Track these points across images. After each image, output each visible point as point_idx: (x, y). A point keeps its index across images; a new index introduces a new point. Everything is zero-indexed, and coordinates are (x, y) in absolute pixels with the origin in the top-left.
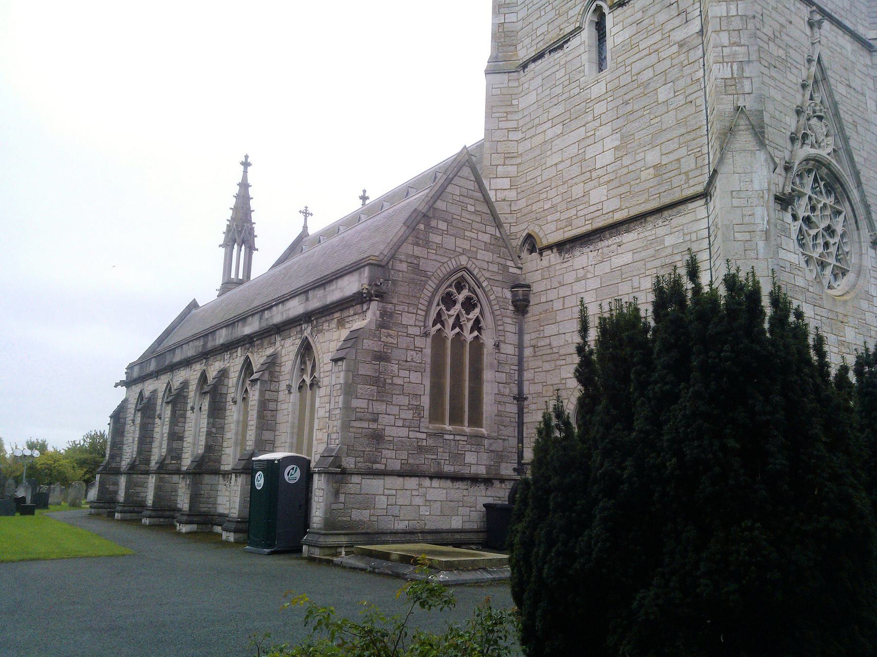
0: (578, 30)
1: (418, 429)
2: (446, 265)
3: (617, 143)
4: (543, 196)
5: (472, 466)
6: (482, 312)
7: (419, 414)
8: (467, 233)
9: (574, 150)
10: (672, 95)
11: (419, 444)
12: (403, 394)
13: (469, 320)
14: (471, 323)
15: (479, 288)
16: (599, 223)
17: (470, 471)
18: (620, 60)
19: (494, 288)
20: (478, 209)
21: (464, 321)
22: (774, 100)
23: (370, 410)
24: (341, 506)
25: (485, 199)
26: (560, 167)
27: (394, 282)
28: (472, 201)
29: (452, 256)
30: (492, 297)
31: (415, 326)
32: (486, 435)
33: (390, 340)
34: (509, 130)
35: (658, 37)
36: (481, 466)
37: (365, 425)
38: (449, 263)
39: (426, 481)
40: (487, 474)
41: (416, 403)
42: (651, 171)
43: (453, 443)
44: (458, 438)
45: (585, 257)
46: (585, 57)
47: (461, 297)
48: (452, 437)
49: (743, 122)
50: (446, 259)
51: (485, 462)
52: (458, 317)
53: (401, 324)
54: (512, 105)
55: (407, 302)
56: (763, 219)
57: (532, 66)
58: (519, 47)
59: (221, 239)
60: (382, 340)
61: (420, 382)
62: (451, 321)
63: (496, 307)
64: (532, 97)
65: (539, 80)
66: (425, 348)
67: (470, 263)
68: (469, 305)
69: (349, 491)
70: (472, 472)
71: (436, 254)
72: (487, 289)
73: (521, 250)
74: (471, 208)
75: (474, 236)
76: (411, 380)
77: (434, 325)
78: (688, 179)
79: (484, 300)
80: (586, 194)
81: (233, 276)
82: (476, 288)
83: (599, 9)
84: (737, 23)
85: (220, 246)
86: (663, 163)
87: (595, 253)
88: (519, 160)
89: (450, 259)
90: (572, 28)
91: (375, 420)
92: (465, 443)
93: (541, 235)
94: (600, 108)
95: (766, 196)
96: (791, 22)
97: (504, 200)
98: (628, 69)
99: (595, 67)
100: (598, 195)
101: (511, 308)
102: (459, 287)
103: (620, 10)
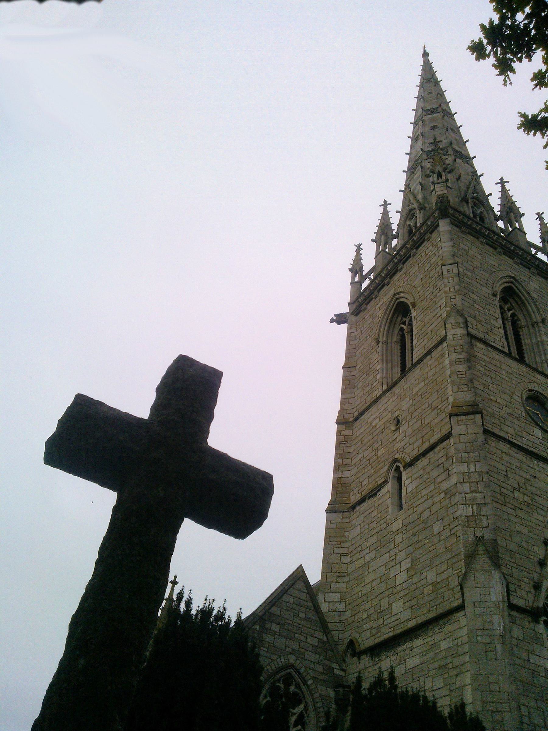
0: (386, 482)
2: (275, 662)
3: (410, 565)
4: (362, 608)
8: (297, 636)
9: (382, 570)
10: (442, 529)
15: (304, 685)
16: (399, 630)
18: (410, 503)
19: (318, 686)
20: (309, 616)
22: (521, 533)
25: (315, 608)
26: (374, 584)
28: (303, 609)
29: (281, 655)
30: (316, 695)
34: (341, 555)
35: (432, 487)
38: (279, 660)
42: (431, 587)
45: (388, 660)
46: (389, 502)
49: (481, 548)
54: (344, 536)
56: (500, 626)
57: (358, 507)
58: (351, 494)
63: (319, 704)
64: (358, 531)
65: (362, 517)
67: (298, 662)
71: (268, 652)
72: (311, 687)
74: (302, 615)
75: (303, 638)
78: (454, 593)
80: (390, 606)
83: (398, 468)
84: (475, 477)
86: (438, 581)
87: (395, 657)
88: (347, 579)
89: (280, 657)
90: (382, 480)
93: (360, 641)
94: (398, 538)
95: (501, 607)
96: (535, 477)
97: (335, 611)
98: (415, 510)
99: (396, 508)
100: (397, 607)
103: (410, 469)
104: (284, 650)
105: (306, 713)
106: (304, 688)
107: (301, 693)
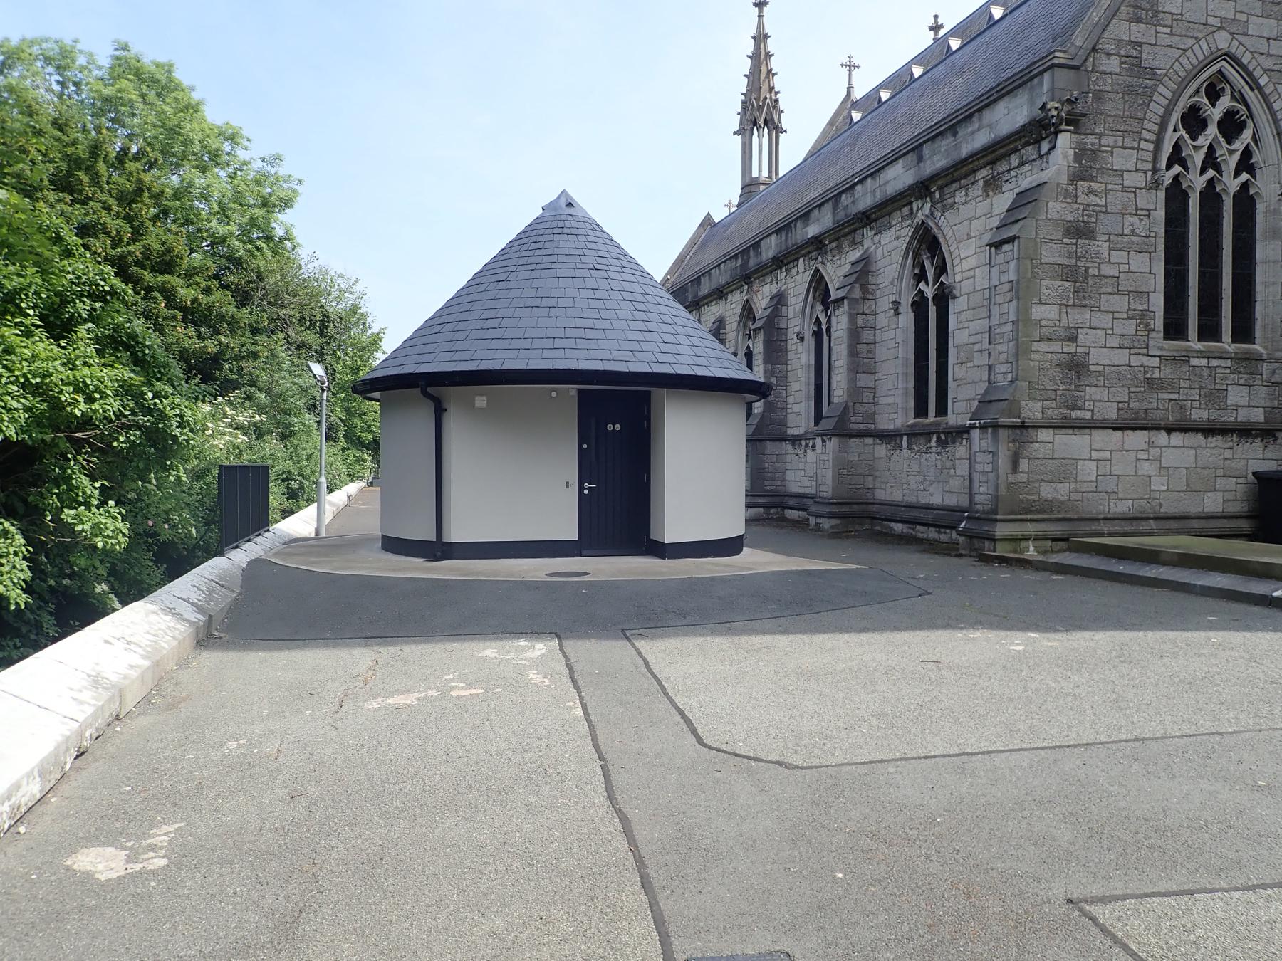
1: (1145, 351)
2: (1189, 53)
5: (1240, 409)
6: (1255, 138)
7: (1147, 325)
11: (1148, 376)
12: (1118, 292)
13: (1231, 152)
14: (1237, 156)
15: (1252, 90)
17: (1236, 418)
21: (1222, 155)
23: (1064, 323)
24: (1024, 477)
27: (1098, 96)
29: (1200, 35)
31: (1137, 171)
32: (1265, 357)
33: (1093, 199)
36: (1256, 409)
37: (1056, 347)
38: (1196, 47)
39: (1160, 436)
40: (1266, 422)
41: (1140, 307)
43: (1206, 372)
44: (1214, 363)
47: (1216, 113)
48: (1204, 362)
51: (1263, 403)
52: (1211, 149)
53: (1112, 170)
55: (1122, 128)
59: (735, 123)
60: (1079, 201)
61: (1148, 271)
62: (1199, 157)
66: (1155, 209)
67: (1235, 43)
68: (1231, 126)
69: (1034, 454)
70: (1239, 420)
71: (1171, 34)
72: (1267, 91)
77: (1169, 167)
81: (755, 174)
85: (735, 133)
89: (1198, 40)
91: (1073, 339)
92: (1228, 371)
102: (1213, 94)
104: (1204, 25)
105: (1257, 145)
106: (1251, 96)
107: (1244, 108)
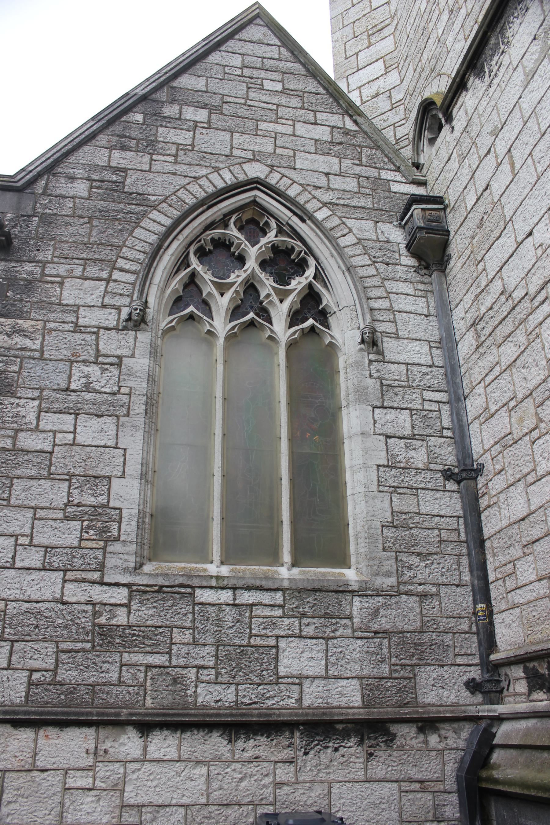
1: (96, 576)
2: (202, 182)
5: (306, 683)
7: (105, 530)
11: (102, 620)
12: (50, 476)
15: (303, 221)
17: (300, 700)
19: (350, 223)
25: (308, 70)
31: (104, 306)
32: (354, 586)
36: (344, 682)
39: (123, 738)
40: (366, 705)
41: (89, 500)
43: (230, 615)
44: (246, 597)
48: (226, 596)
50: (204, 171)
51: (355, 669)
53: (59, 304)
55: (84, 255)
61: (111, 443)
66: (133, 356)
70: (306, 702)
73: (417, 150)
76: (80, 439)
79: (321, 246)
82: (295, 221)
92: (279, 612)
101: (409, 261)
105: (326, 286)
106: (304, 229)
107: (299, 243)
